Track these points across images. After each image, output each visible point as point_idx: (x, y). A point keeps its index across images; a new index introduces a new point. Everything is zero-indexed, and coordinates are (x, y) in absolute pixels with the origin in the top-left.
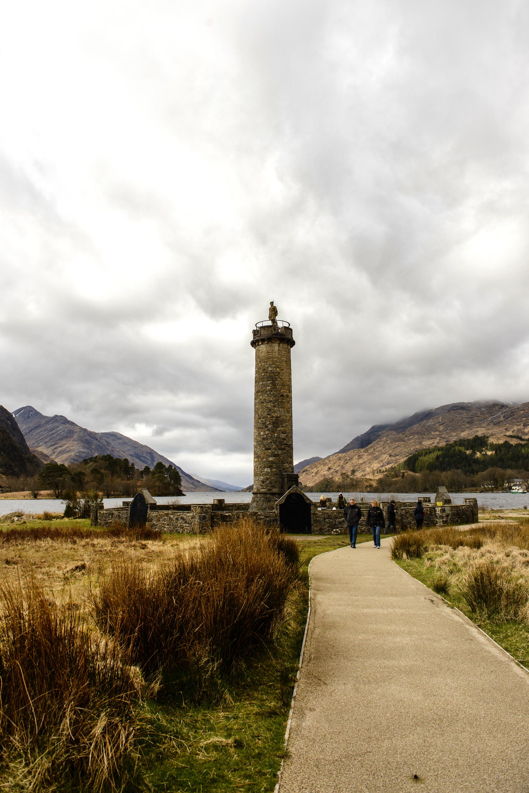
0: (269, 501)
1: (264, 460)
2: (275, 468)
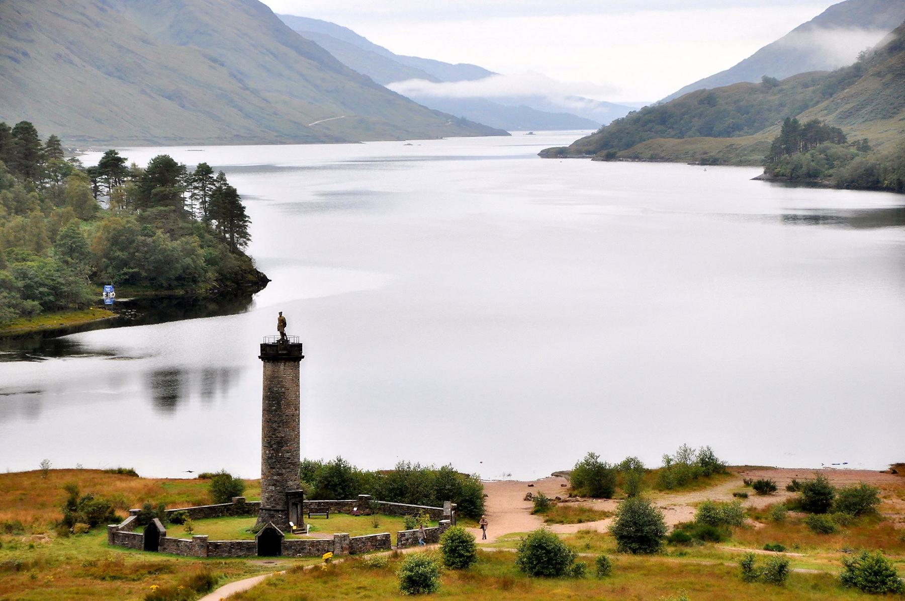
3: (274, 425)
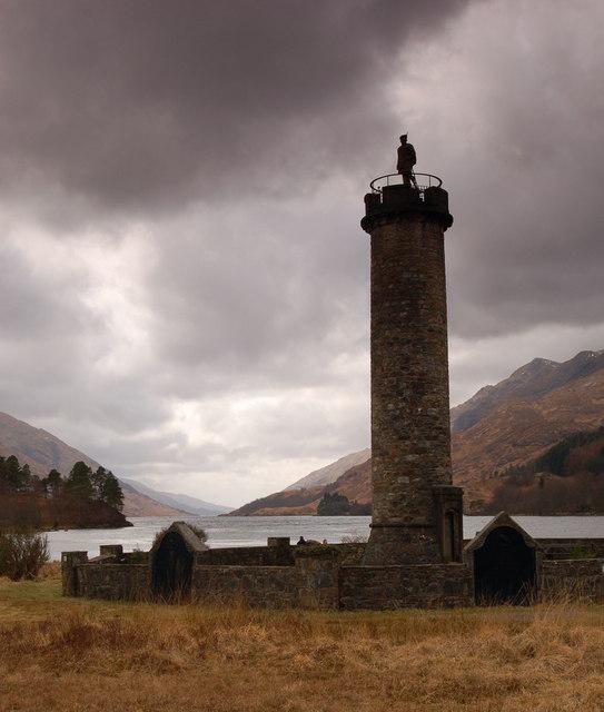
0: (408, 540)
1: (396, 460)
2: (419, 475)
3: (406, 350)
